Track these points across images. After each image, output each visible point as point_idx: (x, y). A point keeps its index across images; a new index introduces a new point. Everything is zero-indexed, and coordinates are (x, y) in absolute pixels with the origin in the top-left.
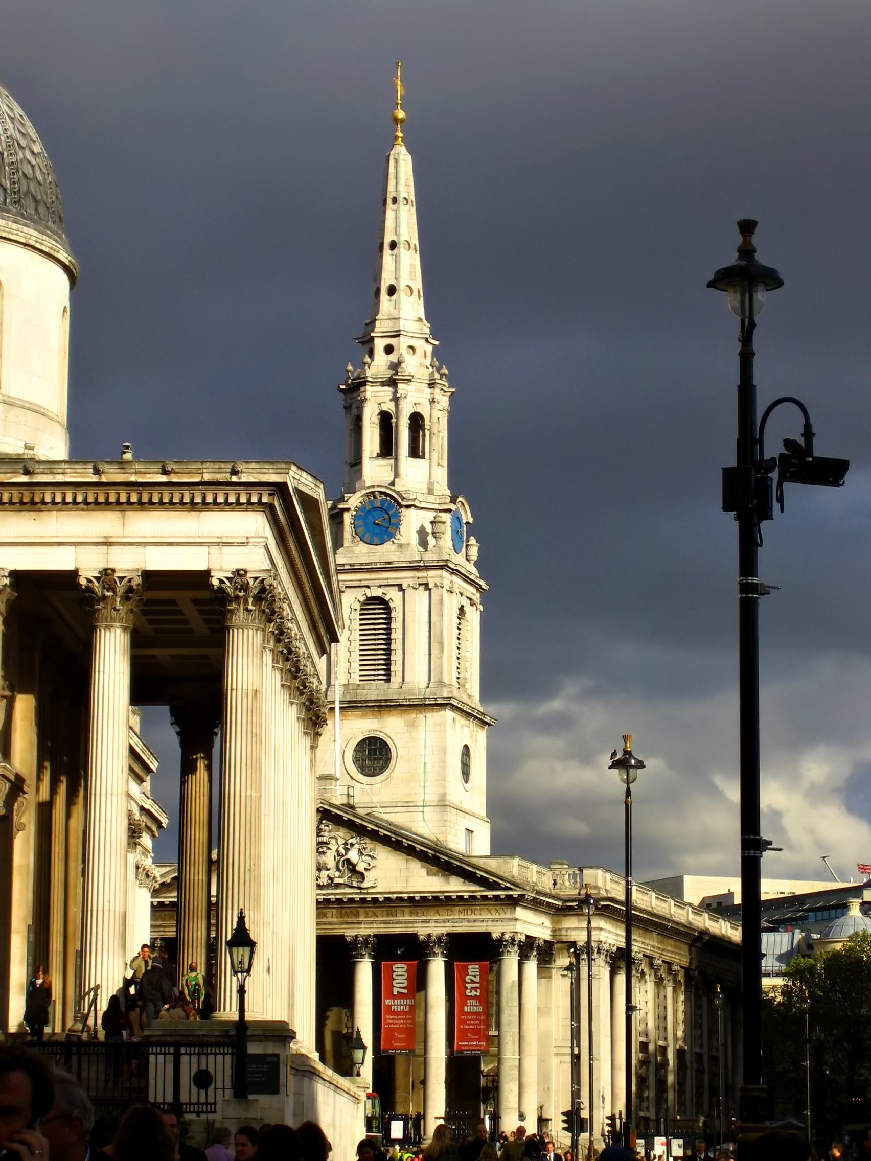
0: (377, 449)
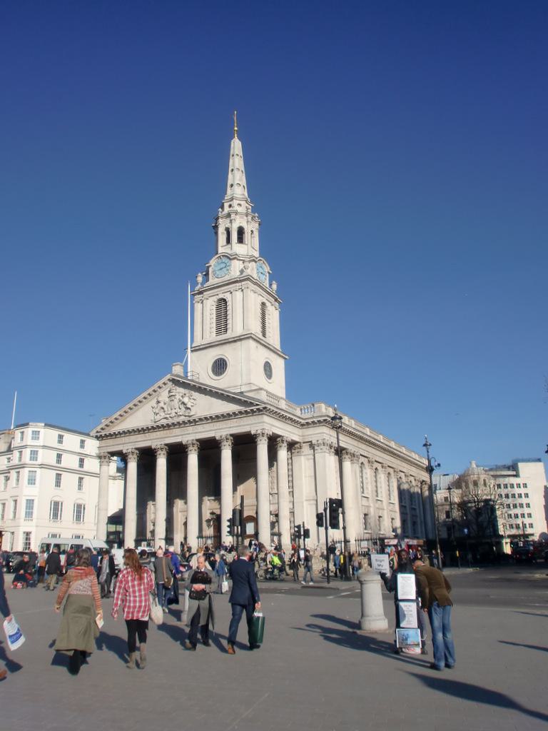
0: (225, 243)
